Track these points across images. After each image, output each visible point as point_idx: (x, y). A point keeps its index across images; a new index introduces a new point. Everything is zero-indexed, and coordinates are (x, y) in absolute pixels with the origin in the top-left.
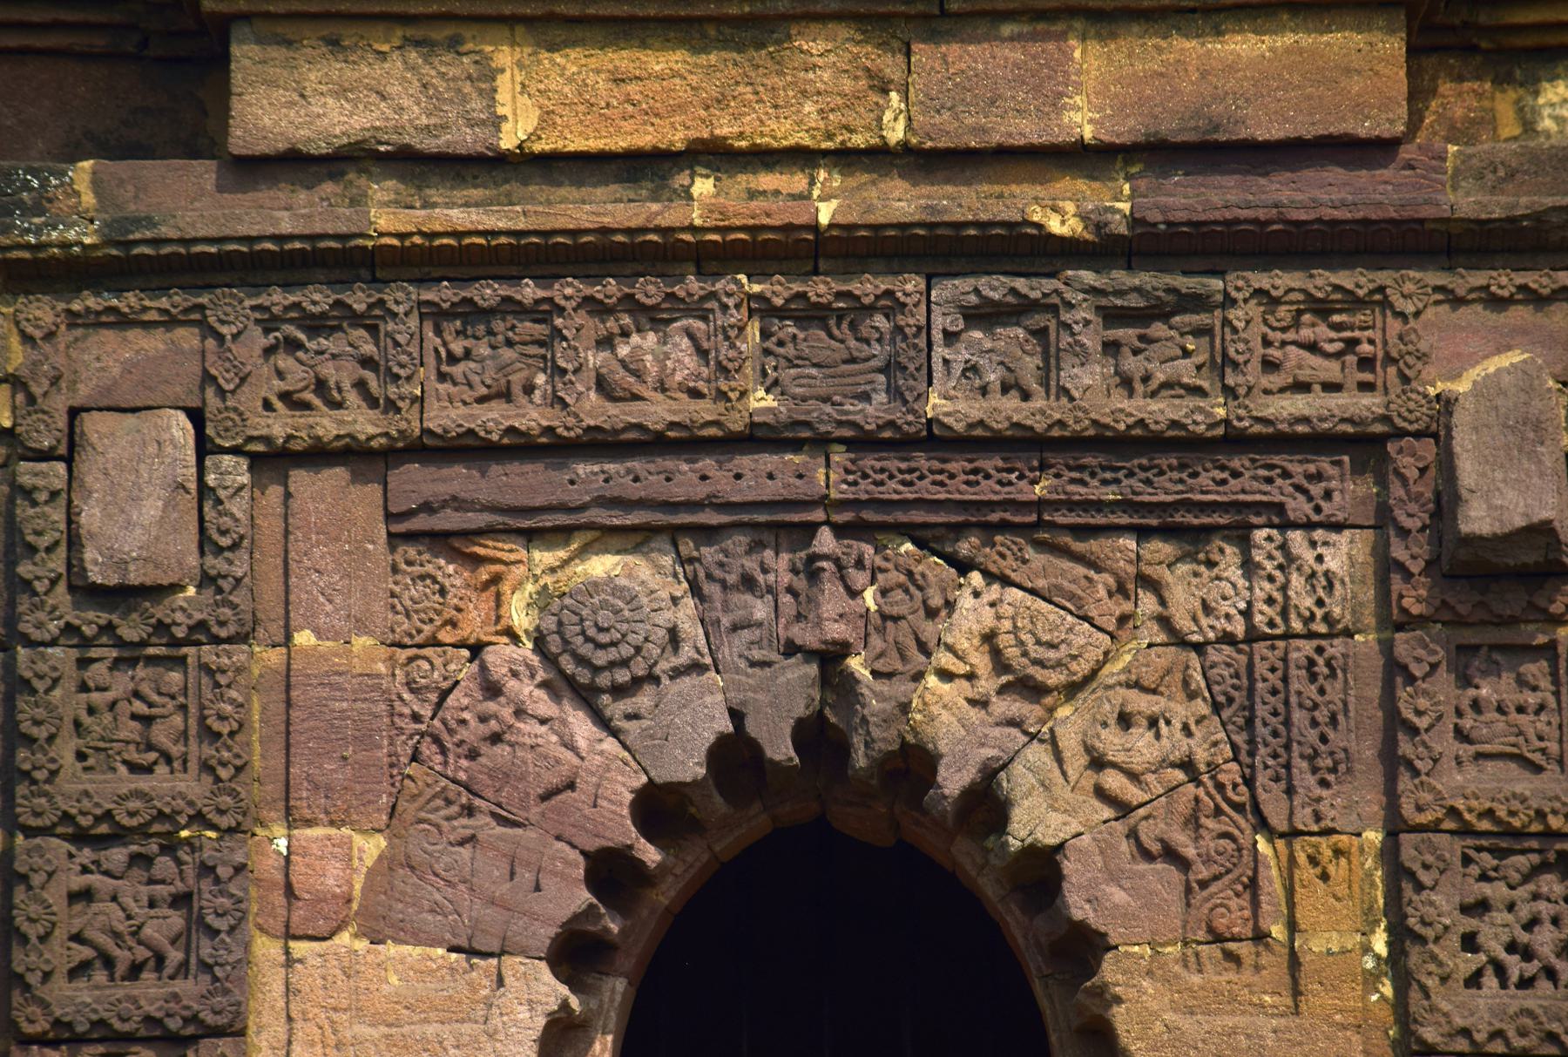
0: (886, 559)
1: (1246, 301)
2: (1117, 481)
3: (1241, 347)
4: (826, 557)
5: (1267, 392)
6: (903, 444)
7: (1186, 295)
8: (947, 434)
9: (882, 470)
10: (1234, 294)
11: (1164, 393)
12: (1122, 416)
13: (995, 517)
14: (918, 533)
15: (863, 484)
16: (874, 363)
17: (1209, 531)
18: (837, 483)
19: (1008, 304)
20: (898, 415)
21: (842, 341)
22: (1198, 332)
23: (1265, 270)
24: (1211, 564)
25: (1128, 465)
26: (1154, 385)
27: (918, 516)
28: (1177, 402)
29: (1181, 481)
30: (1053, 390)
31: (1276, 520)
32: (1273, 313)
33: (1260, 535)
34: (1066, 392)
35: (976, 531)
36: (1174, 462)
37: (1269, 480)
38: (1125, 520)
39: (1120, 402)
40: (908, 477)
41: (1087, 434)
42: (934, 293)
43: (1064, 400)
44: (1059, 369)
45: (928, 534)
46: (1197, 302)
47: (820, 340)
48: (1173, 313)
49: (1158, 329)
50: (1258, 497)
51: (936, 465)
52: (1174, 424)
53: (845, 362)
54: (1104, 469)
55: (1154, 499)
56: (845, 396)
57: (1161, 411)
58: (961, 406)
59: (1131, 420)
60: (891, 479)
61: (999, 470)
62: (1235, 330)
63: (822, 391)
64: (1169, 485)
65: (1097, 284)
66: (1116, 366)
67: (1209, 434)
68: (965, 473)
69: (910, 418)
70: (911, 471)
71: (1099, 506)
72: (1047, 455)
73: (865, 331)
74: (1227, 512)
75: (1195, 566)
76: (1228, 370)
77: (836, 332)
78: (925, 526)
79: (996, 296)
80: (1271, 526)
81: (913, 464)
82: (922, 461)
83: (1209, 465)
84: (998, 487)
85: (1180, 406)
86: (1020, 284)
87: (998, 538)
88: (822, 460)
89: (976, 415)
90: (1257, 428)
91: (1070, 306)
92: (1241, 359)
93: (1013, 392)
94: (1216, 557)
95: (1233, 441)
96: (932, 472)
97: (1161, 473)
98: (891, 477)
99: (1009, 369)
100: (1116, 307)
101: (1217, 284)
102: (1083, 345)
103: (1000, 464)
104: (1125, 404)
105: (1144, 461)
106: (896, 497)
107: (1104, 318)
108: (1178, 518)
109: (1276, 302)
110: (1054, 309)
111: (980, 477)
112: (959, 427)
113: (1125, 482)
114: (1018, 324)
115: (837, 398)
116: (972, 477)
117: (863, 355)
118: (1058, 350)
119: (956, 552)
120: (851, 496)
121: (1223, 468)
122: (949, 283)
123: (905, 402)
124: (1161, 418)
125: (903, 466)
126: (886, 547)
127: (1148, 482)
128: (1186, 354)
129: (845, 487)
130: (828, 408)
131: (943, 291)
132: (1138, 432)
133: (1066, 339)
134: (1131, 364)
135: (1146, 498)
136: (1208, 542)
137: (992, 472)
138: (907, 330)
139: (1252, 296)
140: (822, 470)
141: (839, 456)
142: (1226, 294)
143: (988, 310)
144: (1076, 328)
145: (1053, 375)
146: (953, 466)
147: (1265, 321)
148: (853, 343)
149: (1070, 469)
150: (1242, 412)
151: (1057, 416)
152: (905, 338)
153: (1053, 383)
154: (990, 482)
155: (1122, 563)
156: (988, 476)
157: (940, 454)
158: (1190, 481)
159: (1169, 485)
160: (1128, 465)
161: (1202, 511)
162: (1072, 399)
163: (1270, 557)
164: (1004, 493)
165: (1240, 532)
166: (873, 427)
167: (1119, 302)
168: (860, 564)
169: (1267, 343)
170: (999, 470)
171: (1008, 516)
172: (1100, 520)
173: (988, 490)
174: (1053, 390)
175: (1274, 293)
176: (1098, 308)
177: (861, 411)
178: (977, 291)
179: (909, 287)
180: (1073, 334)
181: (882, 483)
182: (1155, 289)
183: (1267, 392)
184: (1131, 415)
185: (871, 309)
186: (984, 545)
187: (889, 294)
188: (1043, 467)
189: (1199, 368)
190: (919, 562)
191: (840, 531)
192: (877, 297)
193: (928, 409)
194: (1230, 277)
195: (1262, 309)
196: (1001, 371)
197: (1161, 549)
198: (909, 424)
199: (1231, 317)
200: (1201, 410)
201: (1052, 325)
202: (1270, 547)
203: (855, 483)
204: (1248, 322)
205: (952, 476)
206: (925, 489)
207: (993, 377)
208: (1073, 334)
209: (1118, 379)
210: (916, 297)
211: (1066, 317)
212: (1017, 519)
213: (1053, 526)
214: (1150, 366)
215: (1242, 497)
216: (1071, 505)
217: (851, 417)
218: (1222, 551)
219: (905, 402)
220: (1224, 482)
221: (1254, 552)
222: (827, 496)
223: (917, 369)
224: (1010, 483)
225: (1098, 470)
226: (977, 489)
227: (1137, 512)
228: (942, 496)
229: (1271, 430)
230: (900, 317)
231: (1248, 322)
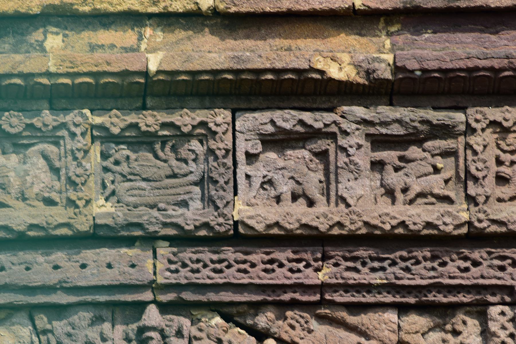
0: (201, 330)
1: (483, 130)
2: (383, 269)
3: (480, 165)
4: (154, 329)
5: (500, 200)
6: (216, 240)
7: (437, 125)
8: (250, 232)
9: (198, 261)
10: (474, 125)
11: (420, 201)
12: (387, 219)
13: (287, 297)
14: (226, 310)
15: (184, 272)
16: (192, 178)
17: (453, 308)
18: (162, 271)
19: (297, 132)
20: (210, 216)
21: (165, 161)
22: (445, 154)
23: (497, 107)
24: (456, 333)
25: (392, 256)
26: (411, 194)
27: (226, 296)
28: (430, 207)
29: (433, 269)
30: (333, 198)
31: (508, 299)
32: (504, 139)
33: (494, 311)
34: (344, 200)
35: (270, 308)
36: (428, 254)
37: (502, 268)
38: (389, 299)
39: (384, 206)
40: (218, 266)
41: (359, 232)
42: (238, 124)
43: (342, 206)
44: (337, 182)
45: (234, 310)
46: (445, 131)
47: (148, 160)
48: (426, 140)
49: (414, 151)
50: (494, 282)
51: (241, 256)
52: (429, 225)
53: (168, 177)
54: (372, 259)
55: (412, 283)
56: (168, 203)
57: (418, 215)
58: (261, 210)
59: (394, 222)
60: (204, 267)
61: (290, 261)
62: (475, 153)
63: (151, 200)
64: (424, 272)
65: (367, 117)
66: (382, 179)
67: (456, 233)
68: (264, 263)
69: (221, 220)
70: (220, 261)
71: (369, 288)
72: (327, 248)
73: (183, 153)
74: (469, 293)
75: (442, 335)
76: (470, 183)
77: (160, 154)
78: (232, 304)
79: (288, 126)
80: (504, 303)
81: (222, 256)
82: (230, 253)
83: (455, 256)
84: (289, 274)
85: (433, 211)
86: (307, 117)
87: (289, 313)
88: (150, 253)
89: (272, 219)
90: (494, 228)
91: (346, 133)
92: (480, 175)
93: (301, 200)
94: (460, 327)
95: (476, 238)
96: (237, 262)
97: (418, 262)
98: (205, 266)
99: (298, 183)
100: (382, 135)
101: (460, 117)
102: (356, 164)
103: (292, 256)
104: (390, 209)
105: (404, 254)
106: (209, 282)
107: (372, 143)
108: (431, 297)
109: (506, 131)
110: (333, 136)
111: (275, 266)
112: (260, 227)
113: (390, 270)
114: (304, 147)
115: (162, 205)
116: (269, 266)
117: (182, 172)
118: (337, 167)
119: (256, 324)
120: (174, 281)
121: (466, 259)
122: (250, 116)
123: (217, 208)
124: (418, 220)
125: (215, 257)
126: (199, 320)
127: (407, 270)
128: (436, 170)
129: (168, 274)
130: (155, 213)
131: (247, 121)
132: (400, 231)
133: (343, 159)
134: (394, 179)
135: (406, 282)
136: (454, 316)
137: (285, 262)
138: (218, 152)
139: (488, 126)
140: (151, 261)
141: (164, 250)
142: (468, 125)
143: (281, 137)
144: (351, 151)
145: (333, 186)
146: (254, 258)
147: (498, 146)
148: (174, 163)
149: (346, 259)
150: (481, 216)
151: (337, 219)
152: (216, 158)
153: (333, 193)
154: (284, 270)
155: (386, 333)
156: (281, 265)
157: (244, 248)
158: (440, 269)
159: (424, 272)
160: (392, 256)
161: (450, 292)
162: (348, 205)
163: (504, 328)
164: (294, 279)
165: (479, 308)
166: (191, 227)
167: (384, 131)
168: (179, 334)
169: (499, 162)
170: (290, 261)
171: (297, 296)
172: (369, 299)
173: (281, 276)
174: (333, 198)
175: (505, 124)
176: (368, 136)
177: (182, 215)
178: (273, 122)
179: (219, 119)
180: (348, 155)
181: (198, 271)
182: (413, 121)
183: (500, 200)
184: (395, 218)
185: (189, 136)
186: (278, 319)
187: (203, 124)
188: (325, 258)
189: (446, 181)
190: (226, 332)
191: (164, 308)
192: (194, 127)
193: (235, 213)
194: (471, 111)
195: (496, 136)
196: (292, 184)
197: (417, 321)
198: (220, 225)
199: (472, 142)
200: (449, 214)
201: (332, 148)
202: (503, 320)
203: (177, 271)
204: (485, 147)
205: (253, 265)
206: (232, 275)
207: (285, 188)
208: (348, 155)
209: (383, 190)
210: (224, 127)
211: (342, 142)
212: (305, 298)
213: (332, 304)
214: (408, 180)
215: (481, 281)
216: (347, 288)
217: (174, 220)
218: (464, 323)
219: (217, 208)
220: (467, 270)
221: (491, 324)
222: (154, 281)
223: (226, 183)
224: (299, 271)
225: (368, 260)
226: (273, 275)
227: (398, 293)
228: (246, 281)
229: (504, 229)
230: (211, 142)
231: (485, 147)
